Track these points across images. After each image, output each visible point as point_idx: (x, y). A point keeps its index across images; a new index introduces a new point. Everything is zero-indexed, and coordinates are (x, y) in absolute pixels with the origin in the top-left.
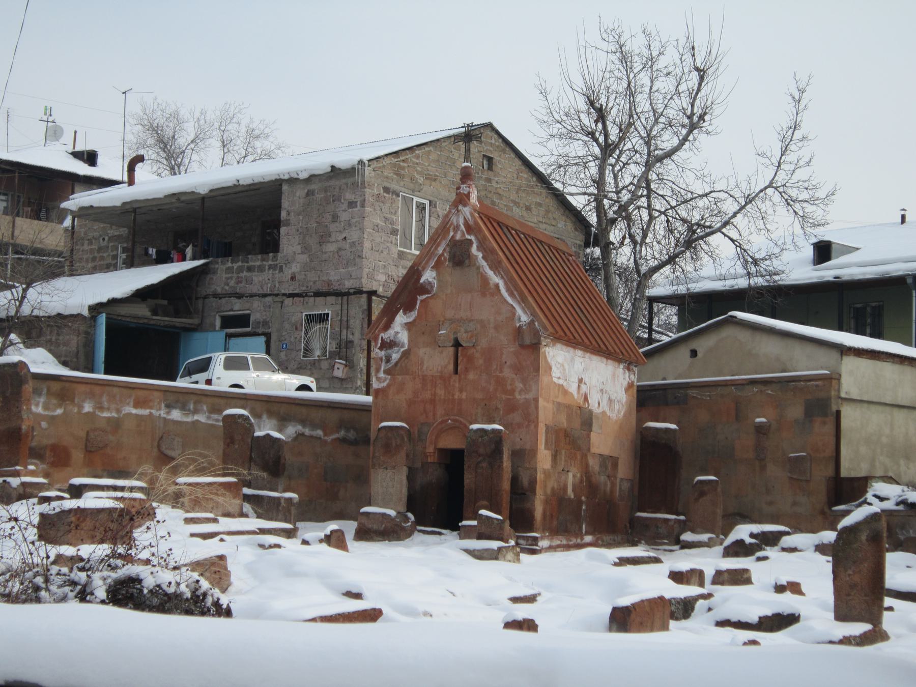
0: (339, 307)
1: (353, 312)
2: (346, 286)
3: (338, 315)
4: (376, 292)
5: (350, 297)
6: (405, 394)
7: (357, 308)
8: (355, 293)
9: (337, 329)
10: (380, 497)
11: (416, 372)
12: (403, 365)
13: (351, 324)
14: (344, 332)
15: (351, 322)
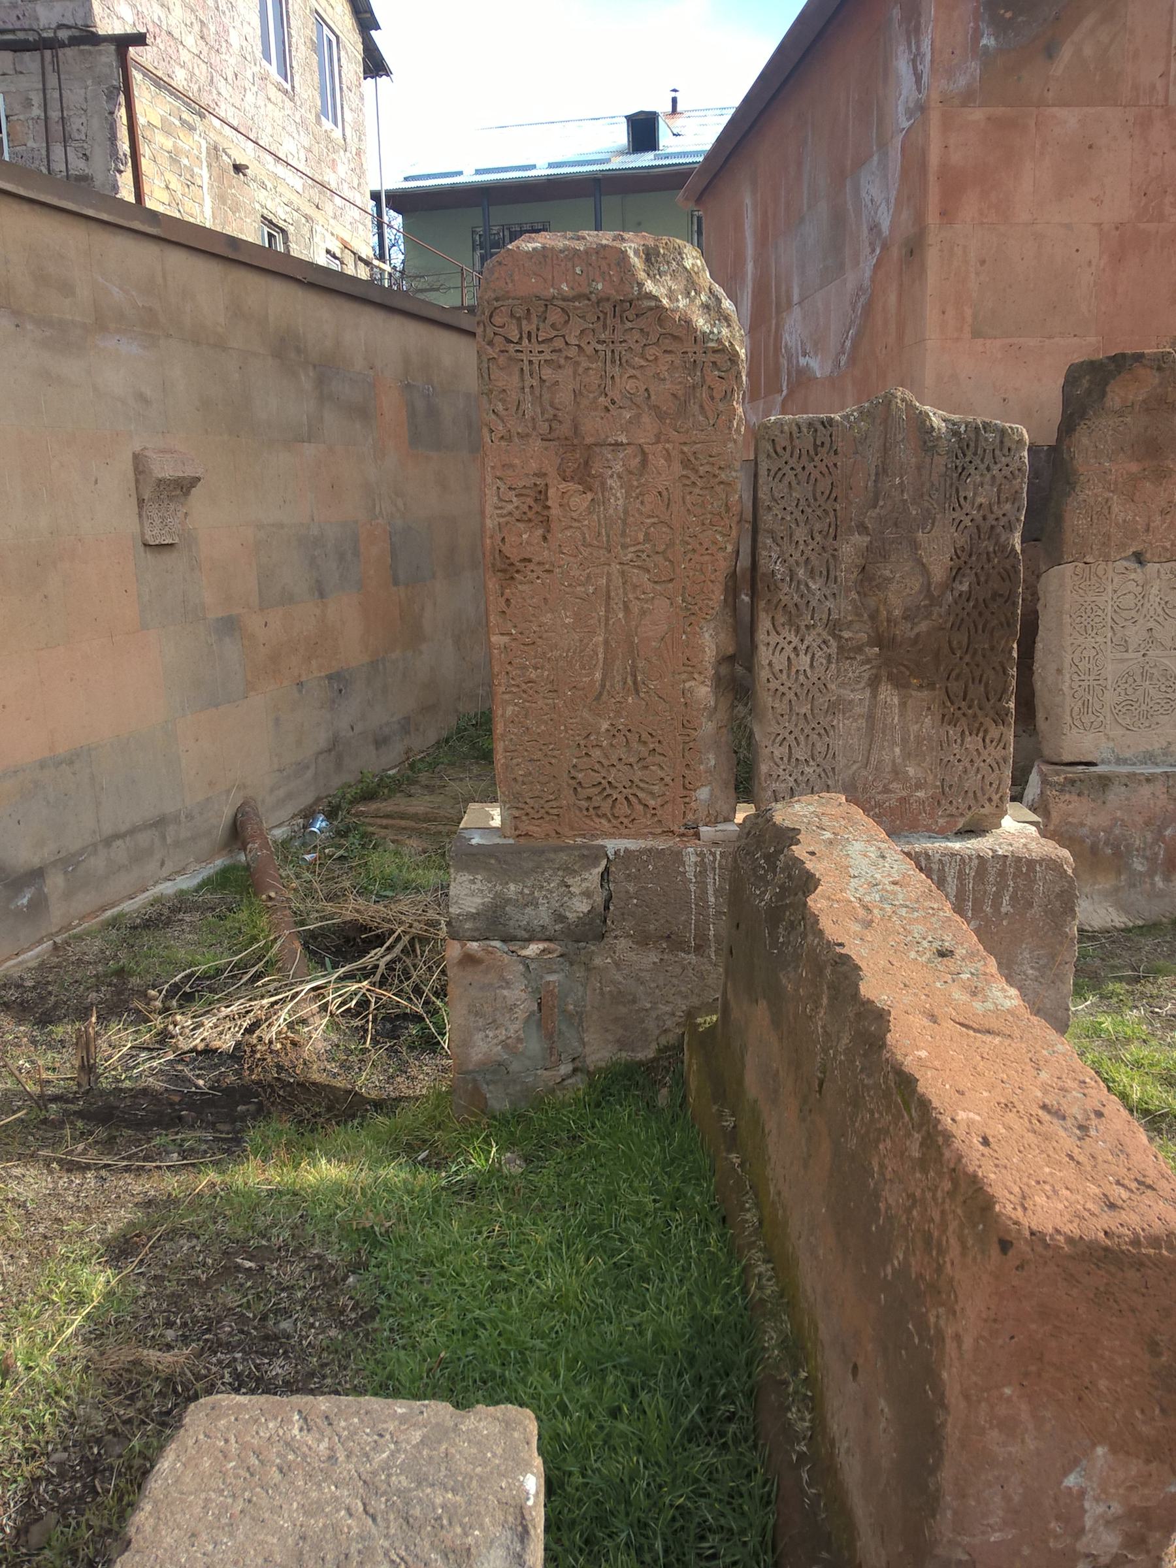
0: (30, 83)
1: (74, 96)
2: (43, 22)
3: (28, 104)
4: (139, 39)
5: (61, 52)
6: (1098, 201)
7: (89, 82)
8: (74, 41)
9: (31, 144)
10: (1110, 697)
11: (1153, 87)
12: (1088, 51)
13: (75, 127)
14: (58, 150)
15: (75, 123)
